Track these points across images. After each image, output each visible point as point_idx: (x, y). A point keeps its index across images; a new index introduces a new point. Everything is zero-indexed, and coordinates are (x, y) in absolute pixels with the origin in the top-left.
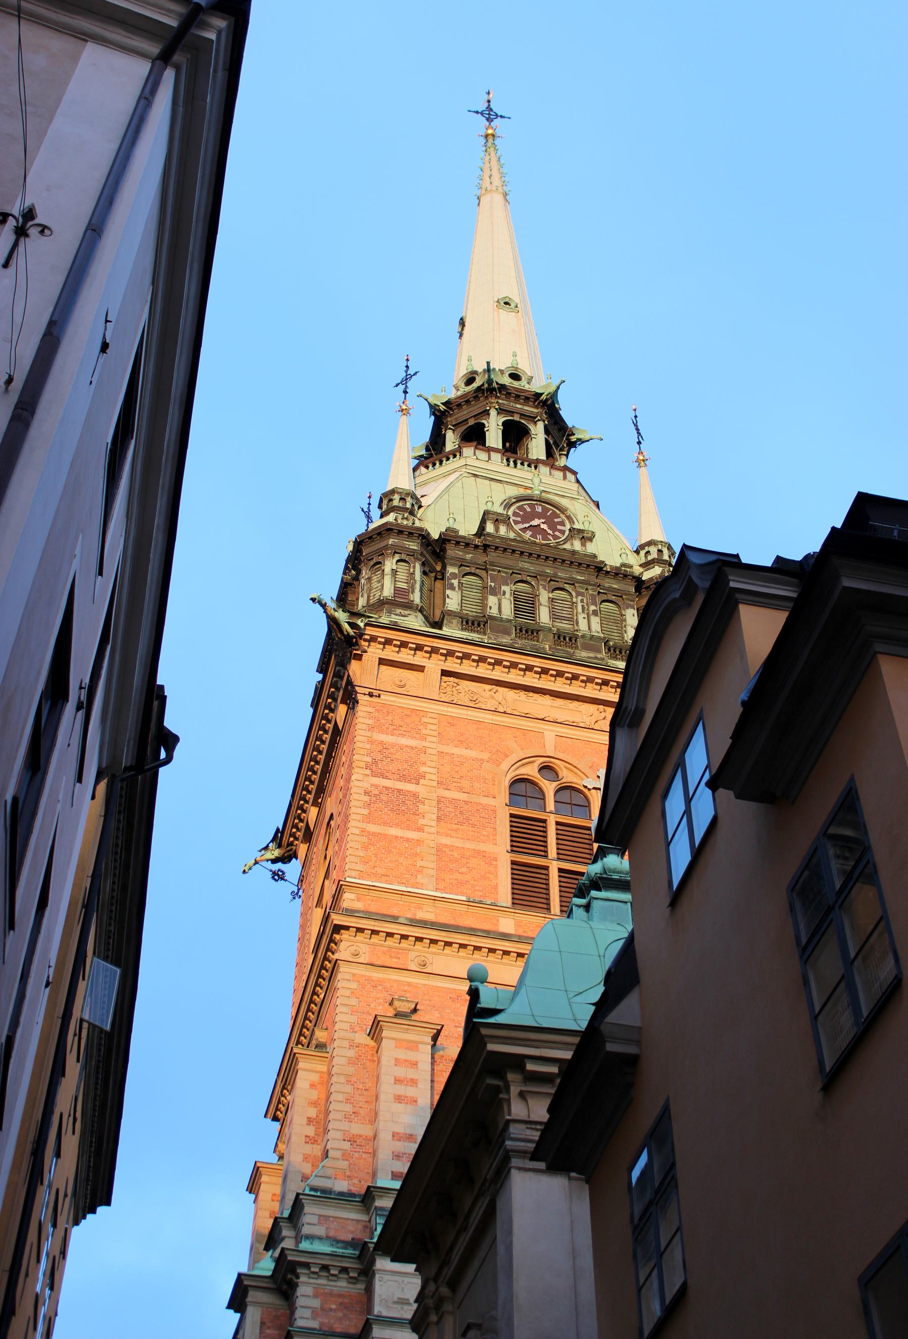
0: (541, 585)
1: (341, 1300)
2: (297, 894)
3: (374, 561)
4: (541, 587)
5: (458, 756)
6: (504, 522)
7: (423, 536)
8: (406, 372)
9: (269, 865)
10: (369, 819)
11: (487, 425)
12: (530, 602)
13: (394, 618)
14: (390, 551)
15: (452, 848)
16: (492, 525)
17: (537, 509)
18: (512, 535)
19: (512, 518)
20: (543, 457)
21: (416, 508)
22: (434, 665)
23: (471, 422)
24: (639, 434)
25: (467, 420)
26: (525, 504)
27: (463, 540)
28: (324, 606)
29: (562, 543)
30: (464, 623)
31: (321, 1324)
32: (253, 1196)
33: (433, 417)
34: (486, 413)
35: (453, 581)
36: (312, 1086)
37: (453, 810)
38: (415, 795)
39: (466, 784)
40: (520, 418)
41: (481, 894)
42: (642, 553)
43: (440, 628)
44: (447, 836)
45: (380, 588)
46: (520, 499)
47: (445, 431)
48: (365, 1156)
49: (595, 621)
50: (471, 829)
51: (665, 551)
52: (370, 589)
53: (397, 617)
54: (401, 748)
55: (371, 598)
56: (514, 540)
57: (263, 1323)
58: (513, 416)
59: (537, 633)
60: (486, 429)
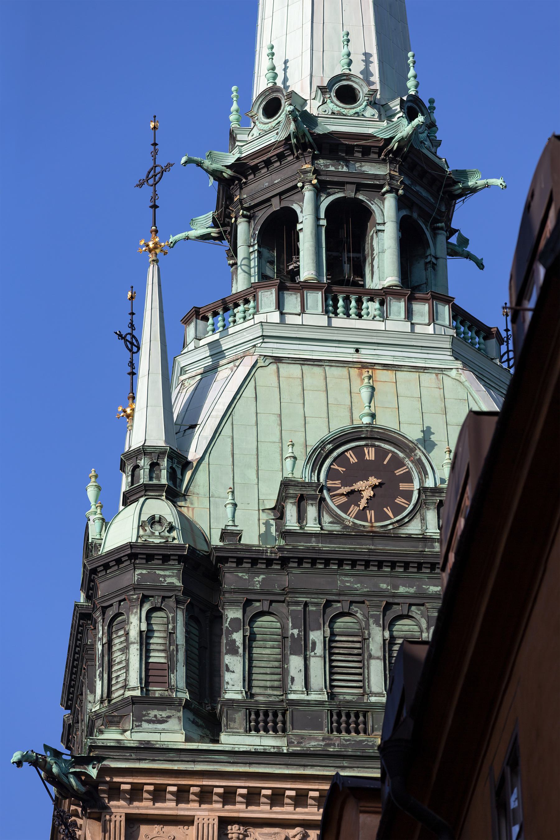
0: (372, 616)
4: (371, 621)
6: (313, 498)
11: (298, 211)
12: (356, 651)
14: (135, 597)
17: (367, 456)
23: (276, 205)
25: (268, 200)
26: (347, 451)
27: (247, 555)
28: (35, 763)
29: (406, 520)
30: (253, 717)
40: (357, 190)
43: (216, 741)
45: (124, 664)
47: (236, 218)
55: (114, 682)
56: (330, 536)
58: (344, 191)
59: (365, 717)
60: (299, 227)
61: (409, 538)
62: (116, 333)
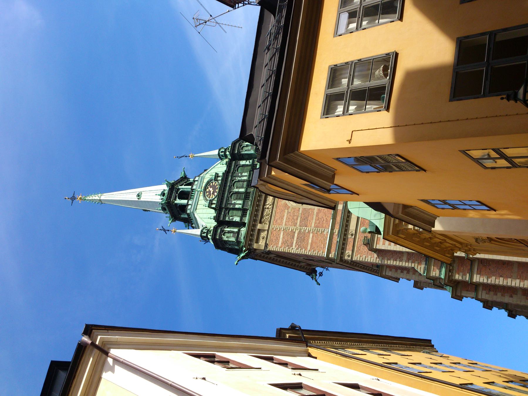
1: (460, 266)
2: (326, 268)
3: (223, 243)
5: (286, 219)
7: (216, 228)
8: (162, 230)
9: (317, 277)
10: (306, 249)
11: (179, 204)
13: (242, 238)
15: (315, 223)
16: (213, 205)
18: (216, 199)
19: (211, 199)
20: (190, 187)
21: (207, 229)
22: (259, 226)
23: (178, 209)
24: (183, 156)
31: (468, 273)
32: (424, 288)
33: (176, 221)
34: (176, 204)
35: (231, 218)
36: (391, 270)
37: (303, 222)
38: (298, 234)
39: (295, 217)
41: (330, 215)
42: (222, 157)
43: (246, 223)
44: (312, 224)
46: (204, 196)
48: (413, 256)
49: (244, 174)
50: (309, 217)
51: (222, 150)
52: (232, 244)
53: (242, 237)
54: (283, 237)
56: (218, 199)
57: (467, 291)
61: (221, 183)
62: (205, 243)
